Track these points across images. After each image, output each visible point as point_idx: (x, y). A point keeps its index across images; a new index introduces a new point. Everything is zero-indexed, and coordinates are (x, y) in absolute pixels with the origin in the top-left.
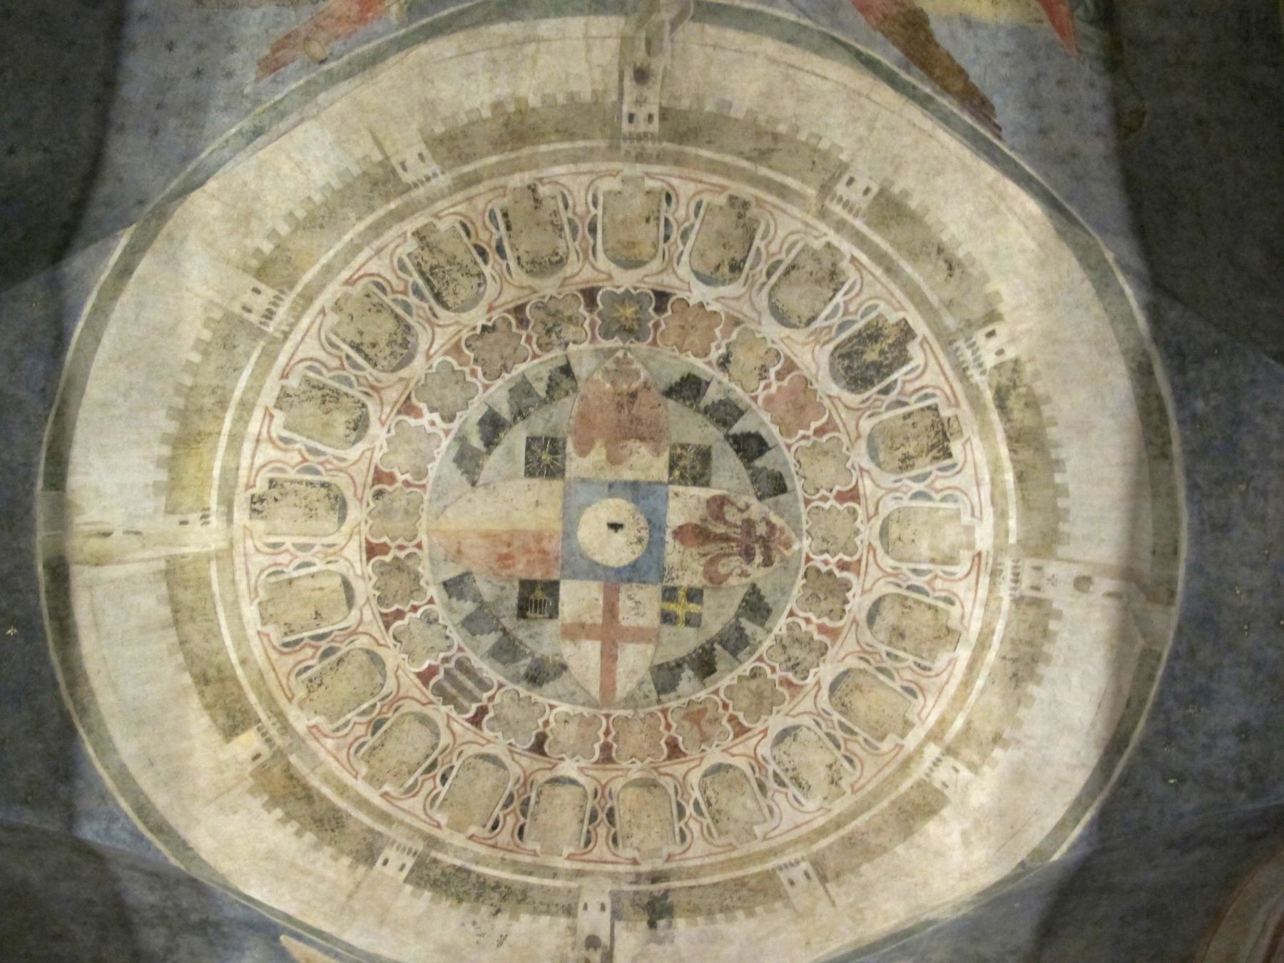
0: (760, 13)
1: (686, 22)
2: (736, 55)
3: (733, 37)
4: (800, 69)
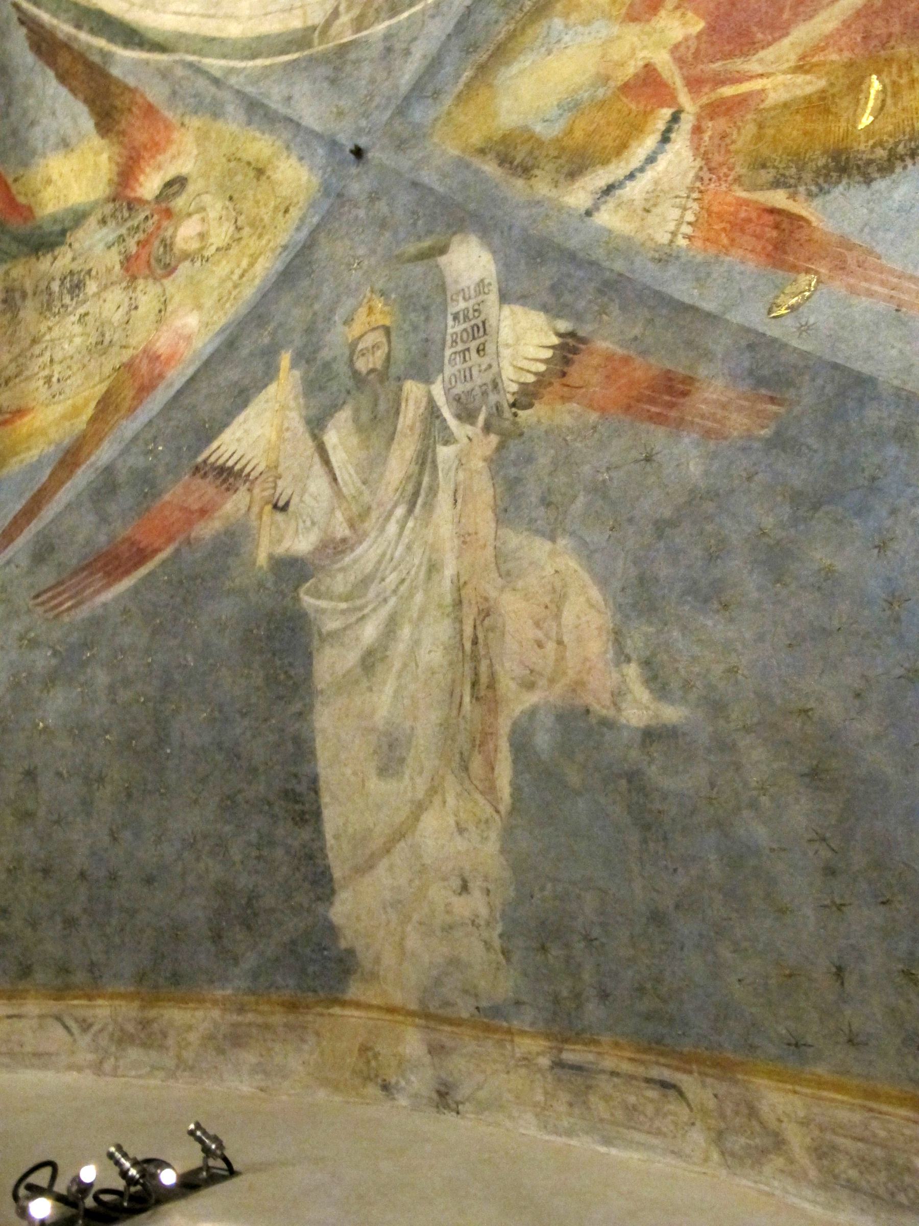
0: (244, 58)
1: (322, 22)
2: (270, 9)
3: (272, 26)
4: (203, 16)
